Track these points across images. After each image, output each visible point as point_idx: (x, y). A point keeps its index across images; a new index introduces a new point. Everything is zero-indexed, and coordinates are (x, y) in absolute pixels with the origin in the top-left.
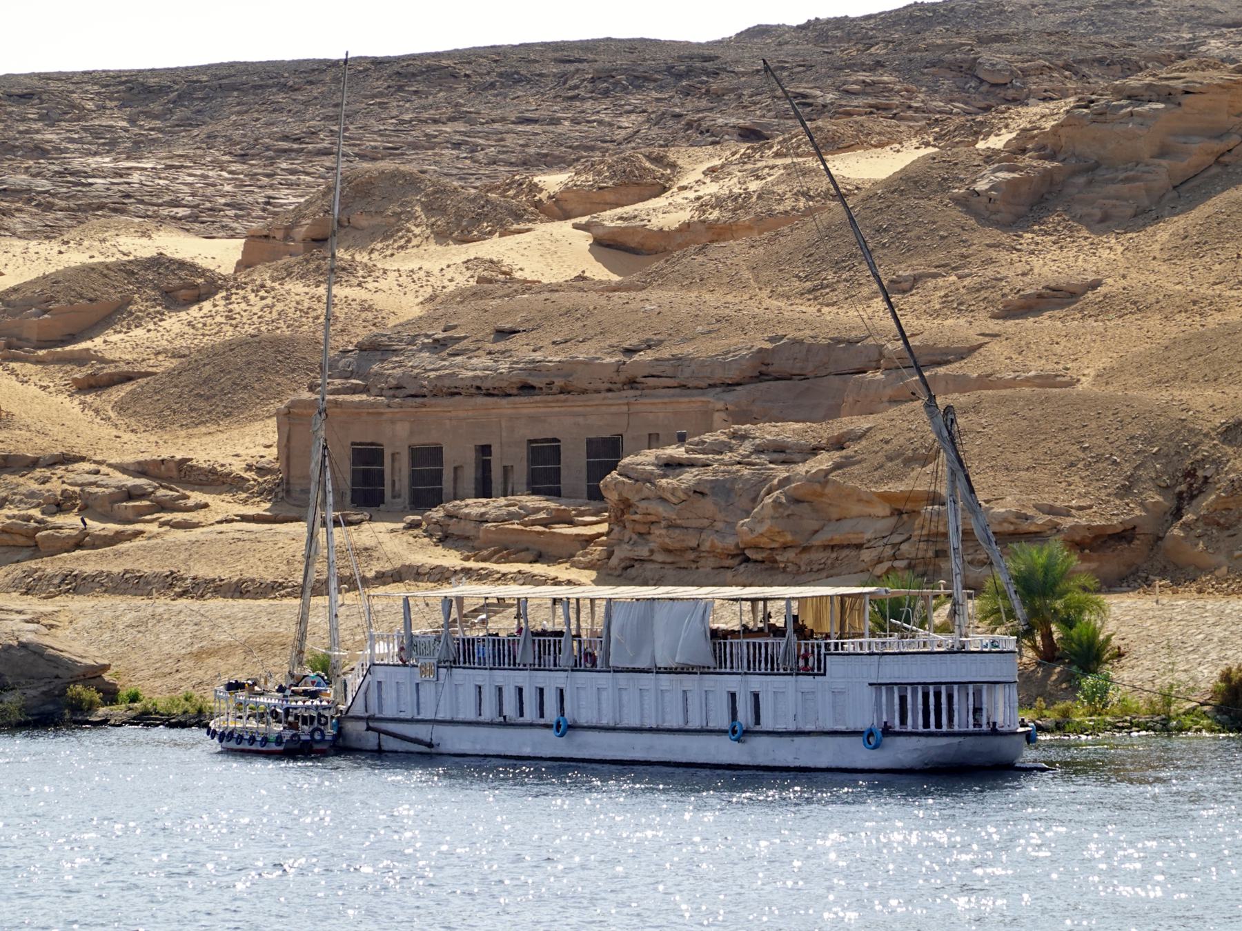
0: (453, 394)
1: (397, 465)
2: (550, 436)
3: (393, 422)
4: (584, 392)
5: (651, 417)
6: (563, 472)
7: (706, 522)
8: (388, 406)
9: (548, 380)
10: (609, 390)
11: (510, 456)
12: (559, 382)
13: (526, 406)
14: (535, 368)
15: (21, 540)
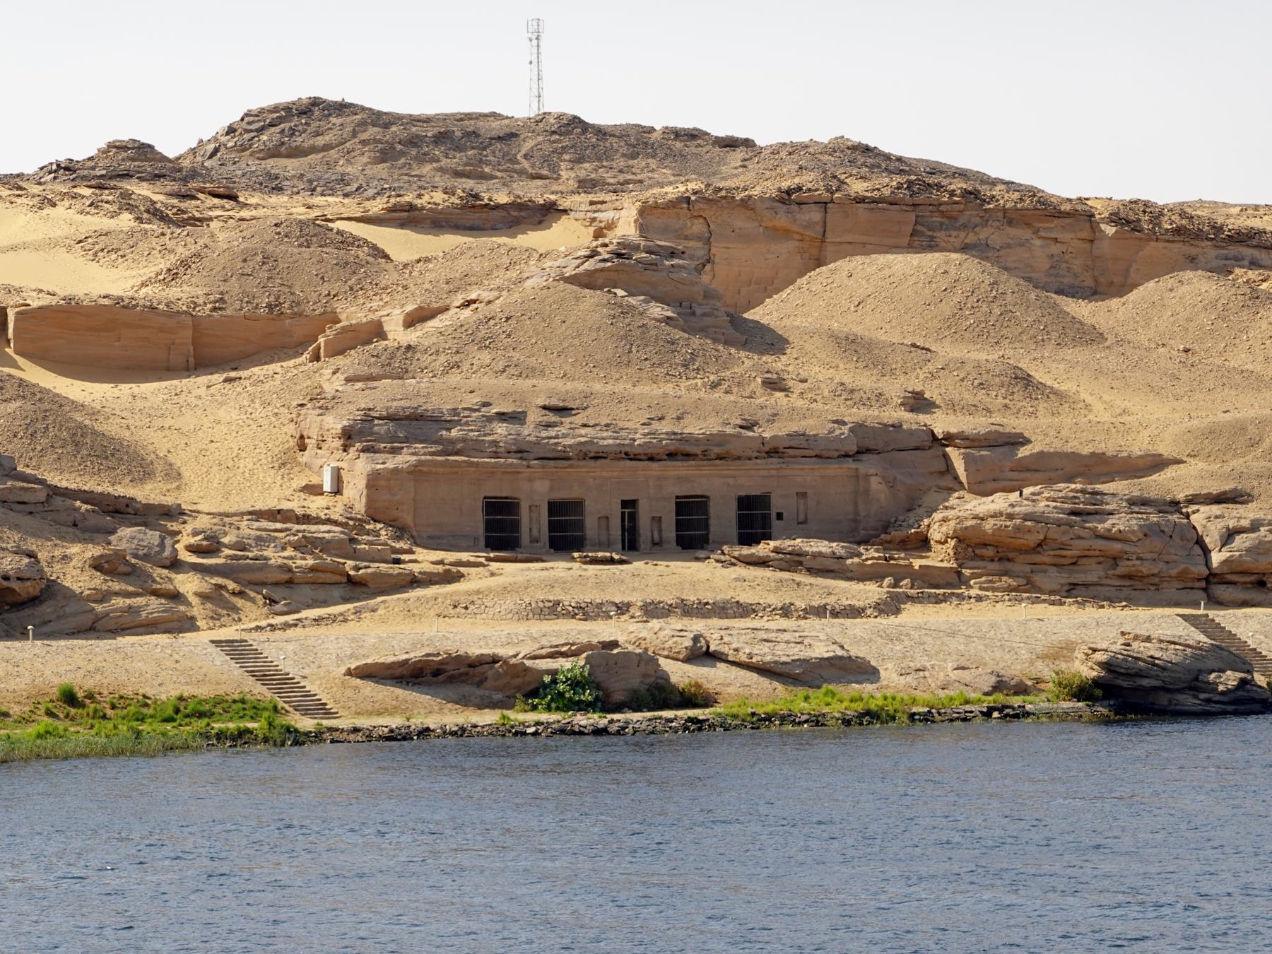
0: (596, 458)
1: (534, 516)
2: (699, 493)
3: (531, 480)
4: (739, 458)
5: (799, 479)
6: (713, 522)
7: (1155, 556)
11: (657, 509)
12: (717, 450)
14: (684, 439)
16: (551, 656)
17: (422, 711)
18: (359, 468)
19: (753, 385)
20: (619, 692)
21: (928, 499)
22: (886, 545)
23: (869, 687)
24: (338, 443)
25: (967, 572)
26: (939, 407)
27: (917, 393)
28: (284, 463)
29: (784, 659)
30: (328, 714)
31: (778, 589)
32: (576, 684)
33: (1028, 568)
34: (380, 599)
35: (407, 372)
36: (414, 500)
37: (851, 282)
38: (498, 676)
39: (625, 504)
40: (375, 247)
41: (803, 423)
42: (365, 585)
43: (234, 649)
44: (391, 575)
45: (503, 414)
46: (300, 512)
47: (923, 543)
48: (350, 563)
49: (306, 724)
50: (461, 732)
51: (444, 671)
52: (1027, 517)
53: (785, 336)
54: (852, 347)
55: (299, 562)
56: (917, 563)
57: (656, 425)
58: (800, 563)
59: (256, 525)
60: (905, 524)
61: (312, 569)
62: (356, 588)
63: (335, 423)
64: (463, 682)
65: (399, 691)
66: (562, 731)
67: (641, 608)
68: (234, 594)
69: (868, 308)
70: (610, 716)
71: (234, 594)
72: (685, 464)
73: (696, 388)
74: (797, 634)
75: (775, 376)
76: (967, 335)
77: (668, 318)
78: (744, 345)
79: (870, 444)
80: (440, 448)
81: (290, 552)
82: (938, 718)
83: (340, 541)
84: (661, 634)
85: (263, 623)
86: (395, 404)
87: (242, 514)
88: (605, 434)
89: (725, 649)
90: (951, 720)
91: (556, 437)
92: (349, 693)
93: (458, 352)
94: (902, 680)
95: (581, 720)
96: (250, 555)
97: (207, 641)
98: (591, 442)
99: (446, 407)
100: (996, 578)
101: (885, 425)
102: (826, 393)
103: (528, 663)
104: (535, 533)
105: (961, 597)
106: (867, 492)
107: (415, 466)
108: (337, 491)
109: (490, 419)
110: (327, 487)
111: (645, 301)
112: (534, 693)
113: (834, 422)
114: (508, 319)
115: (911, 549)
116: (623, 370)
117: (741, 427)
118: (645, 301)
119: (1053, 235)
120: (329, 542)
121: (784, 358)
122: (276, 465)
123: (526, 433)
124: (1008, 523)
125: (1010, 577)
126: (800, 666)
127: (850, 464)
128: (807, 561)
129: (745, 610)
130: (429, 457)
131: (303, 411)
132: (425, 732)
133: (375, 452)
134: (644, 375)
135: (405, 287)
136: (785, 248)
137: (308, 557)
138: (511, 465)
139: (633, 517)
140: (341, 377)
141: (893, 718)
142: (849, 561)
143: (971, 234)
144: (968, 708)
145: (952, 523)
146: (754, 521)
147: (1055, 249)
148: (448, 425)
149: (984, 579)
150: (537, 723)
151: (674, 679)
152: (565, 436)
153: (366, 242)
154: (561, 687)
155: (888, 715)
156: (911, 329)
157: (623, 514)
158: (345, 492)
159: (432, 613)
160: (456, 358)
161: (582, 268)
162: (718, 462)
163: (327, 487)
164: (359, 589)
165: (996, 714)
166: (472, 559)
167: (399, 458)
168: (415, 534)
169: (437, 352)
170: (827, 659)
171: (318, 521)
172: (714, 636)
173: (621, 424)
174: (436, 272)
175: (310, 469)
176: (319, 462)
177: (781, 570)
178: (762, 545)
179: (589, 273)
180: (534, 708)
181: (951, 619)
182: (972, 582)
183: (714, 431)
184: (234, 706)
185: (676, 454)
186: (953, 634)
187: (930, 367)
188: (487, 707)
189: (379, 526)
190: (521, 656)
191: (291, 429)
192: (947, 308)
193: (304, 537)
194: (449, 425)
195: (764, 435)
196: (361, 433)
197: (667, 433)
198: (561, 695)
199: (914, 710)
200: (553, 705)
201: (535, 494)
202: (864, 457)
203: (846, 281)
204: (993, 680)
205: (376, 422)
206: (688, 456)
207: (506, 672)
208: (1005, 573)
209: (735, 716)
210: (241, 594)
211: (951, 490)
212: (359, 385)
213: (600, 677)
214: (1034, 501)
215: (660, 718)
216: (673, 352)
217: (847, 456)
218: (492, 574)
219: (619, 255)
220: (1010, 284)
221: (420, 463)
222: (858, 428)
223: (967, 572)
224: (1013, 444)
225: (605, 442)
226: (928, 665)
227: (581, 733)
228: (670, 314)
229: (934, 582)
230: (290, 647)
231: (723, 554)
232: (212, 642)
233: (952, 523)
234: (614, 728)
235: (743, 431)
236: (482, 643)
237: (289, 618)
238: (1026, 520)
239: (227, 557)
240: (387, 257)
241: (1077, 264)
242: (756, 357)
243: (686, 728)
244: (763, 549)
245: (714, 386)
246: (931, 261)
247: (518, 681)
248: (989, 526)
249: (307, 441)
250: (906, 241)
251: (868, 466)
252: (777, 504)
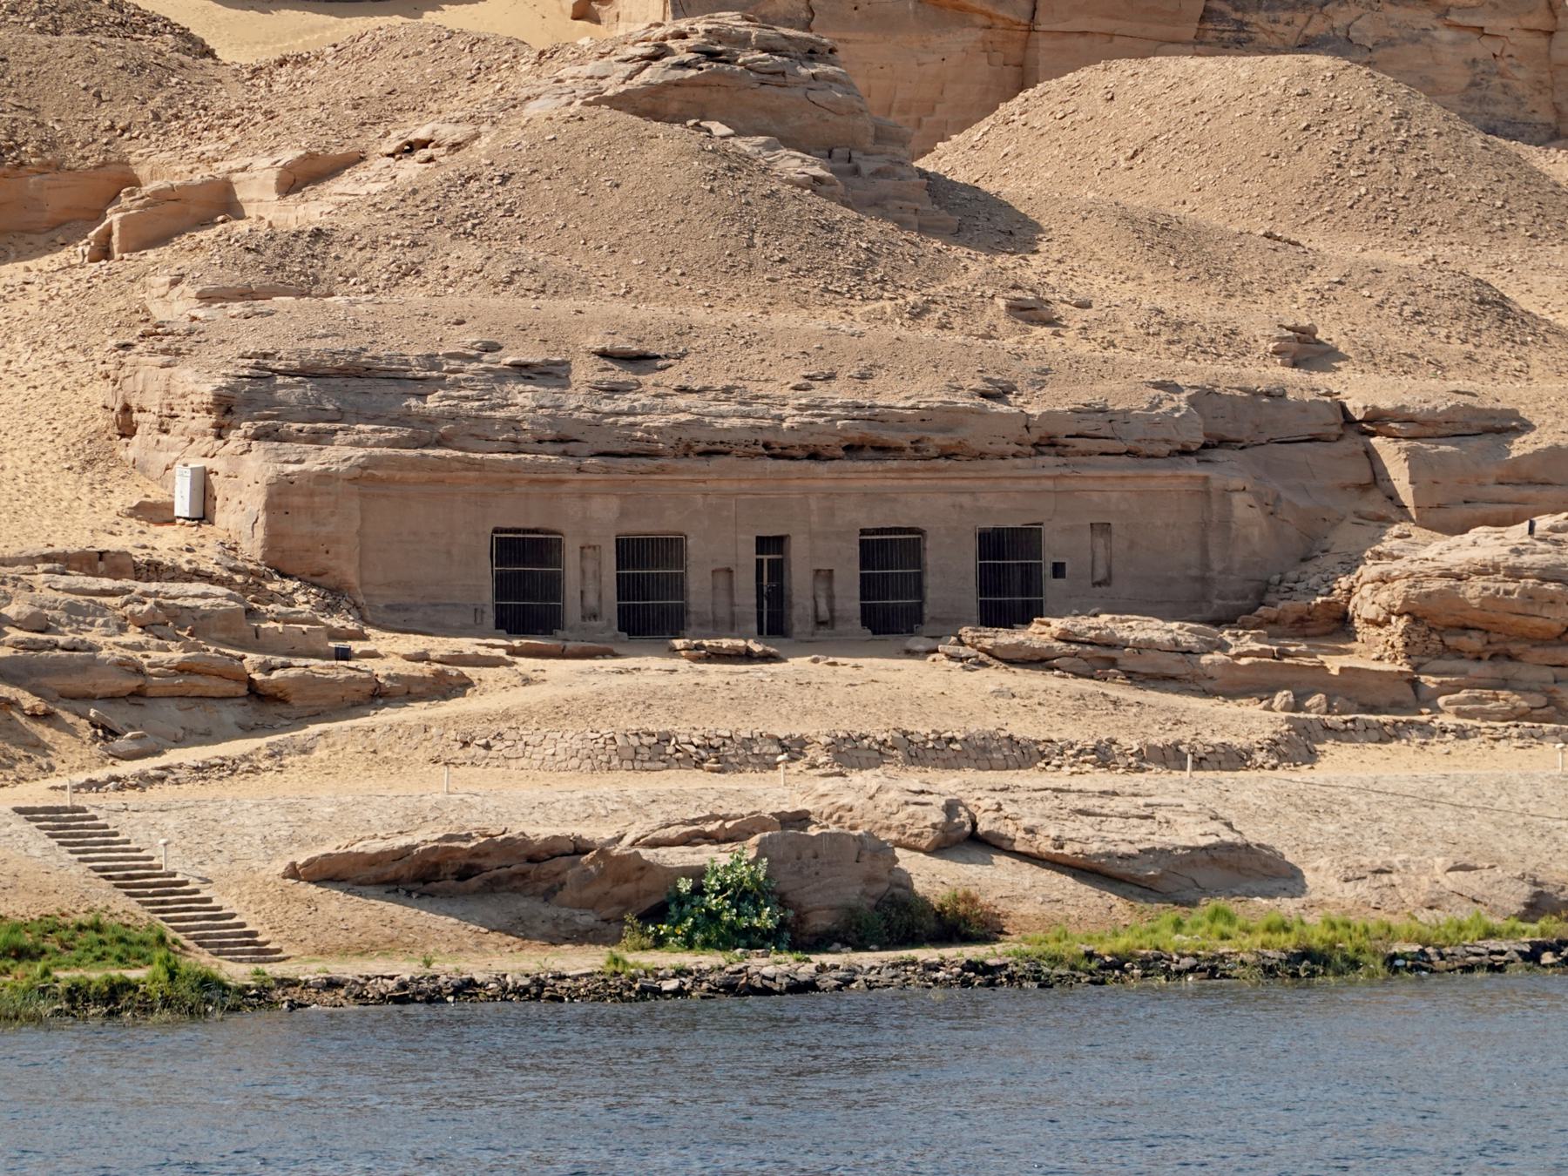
0: (707, 454)
1: (590, 566)
2: (905, 523)
3: (583, 496)
4: (982, 456)
5: (1095, 497)
6: (930, 581)
8: (579, 470)
9: (917, 435)
10: (1014, 456)
12: (940, 439)
13: (866, 475)
14: (877, 417)
15: (230, 687)
16: (687, 840)
17: (444, 948)
18: (249, 473)
19: (989, 312)
20: (826, 912)
21: (1343, 538)
22: (1273, 627)
23: (1288, 906)
24: (206, 422)
25: (1430, 681)
26: (1345, 358)
27: (1303, 331)
28: (91, 460)
29: (1124, 848)
30: (263, 953)
31: (1079, 713)
32: (743, 895)
33: (1548, 674)
34: (315, 729)
35: (316, 281)
36: (359, 533)
37: (1113, 111)
38: (587, 879)
39: (763, 544)
40: (185, 35)
41: (1099, 387)
42: (284, 701)
43: (62, 824)
44: (333, 681)
45: (526, 366)
46: (140, 556)
47: (1340, 625)
48: (252, 659)
49: (237, 972)
50: (536, 990)
51: (479, 870)
52: (1545, 575)
53: (1033, 216)
54: (1163, 237)
55: (156, 656)
56: (1334, 664)
57: (820, 390)
58: (1113, 662)
59: (63, 581)
60: (1300, 586)
61: (182, 669)
62: (266, 706)
63: (198, 382)
64: (515, 890)
65: (393, 909)
66: (730, 988)
67: (828, 748)
68: (34, 716)
69: (1155, 163)
70: (818, 959)
71: (34, 716)
72: (880, 466)
73: (882, 317)
74: (1141, 801)
75: (1030, 296)
76: (1353, 216)
77: (816, 179)
78: (957, 234)
79: (1226, 429)
80: (407, 432)
81: (133, 636)
82: (1440, 964)
83: (228, 615)
84: (883, 799)
85: (100, 774)
86: (315, 345)
87: (32, 560)
88: (724, 407)
89: (1008, 829)
90: (1469, 969)
91: (631, 412)
92: (298, 911)
93: (414, 244)
94: (1350, 892)
95: (769, 965)
96: (61, 640)
97: (7, 809)
98: (698, 423)
99: (414, 352)
100: (1488, 693)
101: (1255, 394)
102: (1130, 330)
103: (647, 854)
104: (591, 600)
105: (1426, 730)
106: (1226, 523)
107: (363, 468)
108: (203, 516)
109: (500, 376)
110: (182, 508)
111: (767, 146)
112: (656, 914)
113: (1158, 386)
114: (505, 179)
115: (1315, 636)
116: (741, 282)
117: (984, 395)
118: (766, 146)
119: (1476, 21)
120: (206, 616)
121: (1035, 260)
122: (76, 463)
123: (572, 403)
124: (1511, 586)
125: (1514, 690)
126: (1155, 863)
127: (1195, 468)
128: (1126, 658)
129: (1025, 754)
130: (390, 451)
131: (130, 359)
132: (466, 989)
133: (282, 440)
134: (780, 290)
135: (270, 115)
136: (960, 41)
137: (171, 645)
138: (546, 466)
139: (778, 571)
140: (188, 290)
141: (1355, 964)
142: (1206, 659)
143: (1317, 19)
144: (1494, 944)
145: (1400, 586)
146: (1010, 581)
147: (1480, 49)
148: (419, 388)
149: (1463, 694)
150: (680, 972)
151: (920, 886)
152: (647, 410)
153: (168, 23)
154: (713, 902)
155: (1345, 958)
156: (1244, 203)
157: (759, 563)
158: (218, 517)
159: (421, 755)
160: (412, 256)
161: (638, 80)
162: (942, 462)
163: (182, 508)
164: (273, 709)
165: (1547, 958)
166: (483, 651)
167: (330, 453)
168: (361, 600)
169: (374, 245)
170: (1205, 848)
171: (175, 574)
172: (985, 804)
173: (753, 388)
174: (327, 86)
175: (144, 471)
176: (164, 458)
177: (1077, 675)
178: (1035, 627)
179: (654, 90)
180: (660, 942)
181: (1422, 773)
182: (1441, 701)
183: (936, 400)
184: (81, 938)
185: (861, 447)
186: (1431, 802)
187: (1316, 279)
188: (567, 940)
189: (291, 585)
190: (627, 840)
191: (102, 393)
192: (1312, 164)
193: (158, 604)
194: (422, 386)
195: (1030, 410)
196: (250, 401)
197: (844, 406)
198: (713, 916)
199: (1396, 948)
200: (698, 937)
201: (592, 524)
202: (1217, 455)
203: (1102, 109)
204: (1526, 890)
205: (280, 380)
206: (884, 450)
207: (602, 873)
208: (1504, 684)
209: (1056, 960)
210: (47, 717)
211: (1384, 521)
212: (236, 308)
213: (786, 882)
214: (1556, 542)
215: (914, 962)
216: (833, 246)
217: (1185, 452)
218: (527, 681)
219: (712, 56)
220: (1432, 117)
221: (373, 462)
222: (1204, 397)
223: (1430, 681)
224: (1499, 431)
225: (727, 423)
226: (1396, 861)
227: (766, 991)
228: (817, 171)
229: (1367, 699)
230: (171, 821)
231: (961, 643)
232: (19, 811)
233: (1400, 586)
234: (829, 980)
235: (989, 403)
236: (537, 815)
237: (149, 765)
238: (1545, 580)
239: (17, 644)
240: (209, 53)
241: (1522, 77)
242: (982, 258)
243: (966, 983)
244: (1038, 634)
245: (918, 313)
246: (1274, 72)
247: (627, 889)
248: (1473, 590)
249: (136, 416)
250: (1190, 31)
251: (1227, 472)
252: (1053, 547)
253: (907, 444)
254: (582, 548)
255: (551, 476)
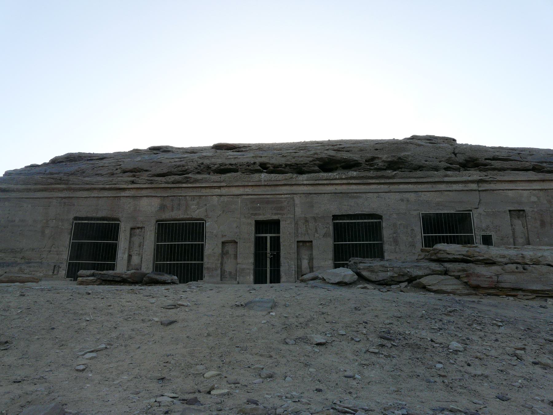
2: (366, 211)
4: (420, 168)
6: (386, 247)
8: (133, 182)
9: (369, 156)
10: (447, 169)
39: (261, 226)
139: (276, 243)
162: (389, 172)
253: (362, 161)
254: (132, 229)
255: (113, 186)
